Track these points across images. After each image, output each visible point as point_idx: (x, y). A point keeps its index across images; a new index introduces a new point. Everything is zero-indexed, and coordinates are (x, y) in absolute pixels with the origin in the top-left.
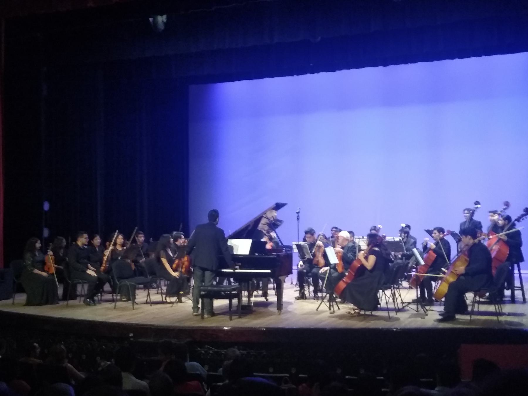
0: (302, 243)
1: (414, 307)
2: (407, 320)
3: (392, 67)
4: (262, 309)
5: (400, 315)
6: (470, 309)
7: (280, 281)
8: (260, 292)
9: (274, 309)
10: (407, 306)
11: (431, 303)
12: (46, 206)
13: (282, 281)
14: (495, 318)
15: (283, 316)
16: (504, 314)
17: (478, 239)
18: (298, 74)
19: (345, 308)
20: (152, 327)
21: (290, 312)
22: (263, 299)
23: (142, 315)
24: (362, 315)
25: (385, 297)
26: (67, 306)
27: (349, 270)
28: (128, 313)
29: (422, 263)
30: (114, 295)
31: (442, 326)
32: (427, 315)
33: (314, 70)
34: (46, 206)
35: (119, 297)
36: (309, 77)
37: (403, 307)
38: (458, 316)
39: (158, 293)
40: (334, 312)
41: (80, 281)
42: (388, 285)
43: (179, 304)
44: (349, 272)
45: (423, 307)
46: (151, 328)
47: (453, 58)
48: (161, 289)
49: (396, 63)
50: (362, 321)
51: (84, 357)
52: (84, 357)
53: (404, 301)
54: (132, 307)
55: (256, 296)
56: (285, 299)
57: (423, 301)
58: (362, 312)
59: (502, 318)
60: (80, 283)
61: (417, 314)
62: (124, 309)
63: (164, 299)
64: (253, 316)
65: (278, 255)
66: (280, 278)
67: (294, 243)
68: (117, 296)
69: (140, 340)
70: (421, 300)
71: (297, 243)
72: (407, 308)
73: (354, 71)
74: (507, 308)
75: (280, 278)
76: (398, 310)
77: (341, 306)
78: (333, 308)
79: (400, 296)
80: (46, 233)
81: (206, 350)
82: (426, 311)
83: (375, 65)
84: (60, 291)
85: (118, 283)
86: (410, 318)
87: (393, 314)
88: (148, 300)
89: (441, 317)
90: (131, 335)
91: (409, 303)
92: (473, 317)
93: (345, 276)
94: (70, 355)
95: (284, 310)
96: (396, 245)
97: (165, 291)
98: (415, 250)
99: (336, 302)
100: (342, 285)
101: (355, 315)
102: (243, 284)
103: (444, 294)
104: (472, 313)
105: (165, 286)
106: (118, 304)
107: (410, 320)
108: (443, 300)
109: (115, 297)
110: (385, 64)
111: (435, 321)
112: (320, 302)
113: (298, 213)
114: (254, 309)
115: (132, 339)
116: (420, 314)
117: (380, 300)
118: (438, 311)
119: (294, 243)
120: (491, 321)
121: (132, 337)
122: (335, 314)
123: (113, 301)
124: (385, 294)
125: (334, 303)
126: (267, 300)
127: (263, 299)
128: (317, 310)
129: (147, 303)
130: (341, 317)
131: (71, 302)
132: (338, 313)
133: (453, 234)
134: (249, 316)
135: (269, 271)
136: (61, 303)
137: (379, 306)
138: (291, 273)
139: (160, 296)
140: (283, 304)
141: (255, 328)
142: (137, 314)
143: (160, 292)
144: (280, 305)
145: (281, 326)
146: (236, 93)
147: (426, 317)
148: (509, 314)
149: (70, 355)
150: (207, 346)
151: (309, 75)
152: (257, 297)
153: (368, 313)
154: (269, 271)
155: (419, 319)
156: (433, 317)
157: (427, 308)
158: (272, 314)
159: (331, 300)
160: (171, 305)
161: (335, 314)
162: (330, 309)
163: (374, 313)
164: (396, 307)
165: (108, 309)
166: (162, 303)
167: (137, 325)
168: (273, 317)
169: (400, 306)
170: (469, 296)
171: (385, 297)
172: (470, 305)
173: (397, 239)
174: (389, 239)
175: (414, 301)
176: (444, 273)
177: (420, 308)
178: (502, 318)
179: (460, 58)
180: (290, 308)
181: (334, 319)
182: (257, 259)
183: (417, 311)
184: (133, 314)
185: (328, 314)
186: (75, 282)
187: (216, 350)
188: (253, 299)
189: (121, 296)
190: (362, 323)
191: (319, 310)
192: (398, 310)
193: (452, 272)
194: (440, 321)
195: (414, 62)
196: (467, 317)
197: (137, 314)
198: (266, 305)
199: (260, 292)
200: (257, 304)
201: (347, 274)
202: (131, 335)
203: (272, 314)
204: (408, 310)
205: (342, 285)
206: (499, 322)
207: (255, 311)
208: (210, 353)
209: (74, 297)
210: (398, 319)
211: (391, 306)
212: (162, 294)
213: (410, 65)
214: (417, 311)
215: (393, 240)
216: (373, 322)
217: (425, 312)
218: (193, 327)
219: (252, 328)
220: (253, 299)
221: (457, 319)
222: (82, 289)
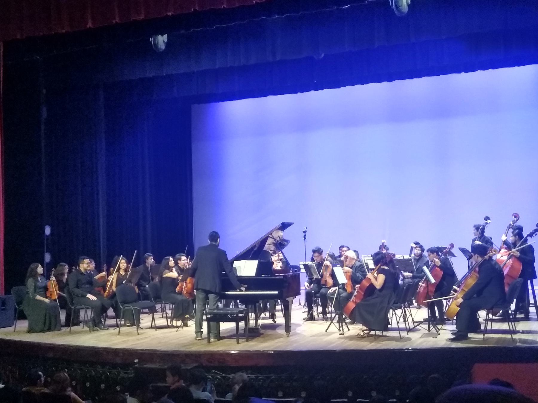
0: (309, 263)
1: (426, 326)
2: (419, 340)
3: (397, 83)
4: (270, 332)
5: (411, 335)
6: (483, 327)
7: (288, 302)
8: (268, 314)
9: (281, 331)
10: (418, 325)
11: (442, 321)
12: (48, 231)
13: (290, 303)
14: (509, 336)
15: (292, 339)
16: (518, 332)
17: (488, 255)
18: (302, 92)
19: (356, 329)
22: (270, 321)
24: (372, 335)
25: (395, 317)
26: (70, 333)
28: (134, 338)
29: (433, 281)
30: (118, 320)
31: (455, 345)
32: (439, 334)
33: (318, 87)
34: (48, 231)
35: (123, 322)
36: (313, 93)
37: (415, 327)
38: (470, 335)
39: (162, 317)
40: (344, 334)
41: (83, 306)
42: (399, 304)
43: (185, 328)
45: (435, 326)
46: (156, 354)
47: (459, 72)
48: (166, 313)
49: (402, 78)
50: (371, 342)
51: (88, 384)
52: (88, 384)
53: (415, 320)
54: (136, 332)
55: (263, 319)
57: (435, 321)
58: (373, 333)
59: (516, 336)
60: (83, 308)
61: (429, 334)
62: (128, 334)
64: (259, 339)
66: (287, 299)
67: (301, 263)
68: (121, 321)
69: (145, 366)
70: (433, 319)
72: (418, 327)
73: (358, 87)
74: (521, 326)
75: (287, 299)
76: (409, 330)
77: (350, 327)
78: (343, 329)
79: (411, 315)
80: (48, 258)
81: (213, 375)
82: (438, 330)
83: (379, 80)
84: (63, 317)
85: (121, 307)
86: (421, 337)
87: (404, 334)
88: (153, 324)
89: (454, 336)
90: (136, 361)
91: (420, 323)
92: (487, 336)
94: (74, 383)
96: (406, 264)
97: (170, 315)
98: (425, 268)
99: (346, 323)
100: (351, 305)
101: (365, 335)
103: (456, 312)
104: (486, 331)
106: (123, 329)
107: (422, 340)
108: (455, 318)
109: (119, 323)
110: (390, 80)
111: (447, 340)
112: (329, 323)
113: (305, 232)
114: (262, 331)
115: (137, 365)
116: (432, 333)
117: (390, 320)
118: (451, 331)
120: (505, 340)
121: (136, 363)
123: (117, 326)
124: (396, 314)
125: (344, 324)
126: (275, 322)
127: (270, 321)
128: (326, 331)
129: (152, 327)
130: (351, 338)
131: (74, 328)
132: (348, 334)
133: (464, 251)
134: (256, 339)
135: (276, 292)
136: (64, 329)
137: (389, 326)
138: (298, 293)
139: (166, 320)
141: (263, 351)
142: (142, 339)
143: (165, 315)
144: (288, 327)
145: (290, 348)
146: (238, 111)
147: (438, 336)
148: (523, 332)
149: (74, 383)
150: (213, 371)
151: (313, 92)
152: (265, 320)
153: (378, 333)
154: (276, 292)
155: (431, 339)
156: (444, 337)
157: (439, 327)
159: (341, 321)
160: (176, 329)
161: (345, 335)
162: (339, 330)
163: (385, 333)
164: (408, 327)
165: (112, 334)
166: (168, 327)
167: (142, 350)
168: (281, 339)
169: (412, 326)
170: (482, 314)
171: (395, 317)
172: (483, 323)
173: (407, 257)
174: (398, 257)
175: (425, 321)
176: (455, 291)
177: (432, 327)
178: (516, 336)
179: (466, 71)
180: (299, 330)
181: (343, 340)
182: (264, 280)
183: (429, 330)
184: (138, 340)
185: (337, 335)
187: (224, 375)
188: (260, 322)
189: (125, 321)
190: (373, 343)
192: (409, 330)
193: (462, 289)
194: (452, 340)
195: (419, 76)
196: (481, 336)
197: (142, 339)
198: (273, 327)
199: (268, 314)
200: (265, 327)
202: (136, 361)
203: (280, 336)
204: (420, 330)
205: (351, 305)
206: (514, 340)
207: (263, 334)
208: (218, 378)
209: (77, 324)
210: (409, 339)
211: (402, 325)
212: (167, 318)
213: (416, 80)
214: (429, 330)
215: (402, 258)
216: (384, 342)
217: (437, 332)
218: (199, 352)
220: (260, 322)
221: (471, 338)
222: (86, 314)
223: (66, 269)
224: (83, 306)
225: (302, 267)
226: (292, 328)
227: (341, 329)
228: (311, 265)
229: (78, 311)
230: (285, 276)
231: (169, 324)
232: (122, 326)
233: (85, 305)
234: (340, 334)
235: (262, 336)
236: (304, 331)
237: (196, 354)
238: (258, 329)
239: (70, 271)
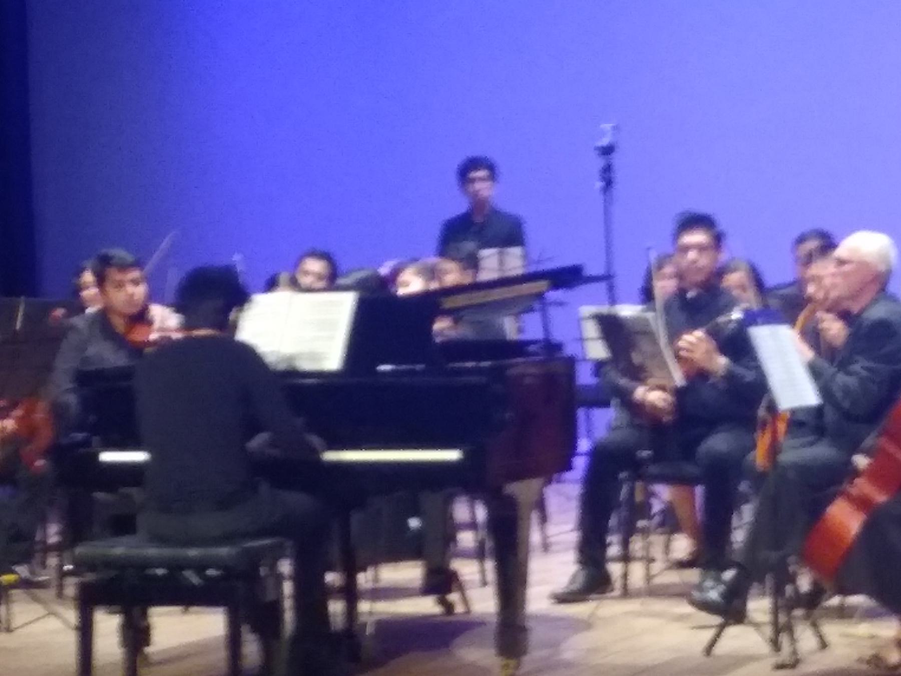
0: (628, 311)
8: (411, 572)
9: (479, 653)
21: (568, 665)
27: (869, 441)
44: (868, 453)
56: (538, 599)
65: (498, 373)
67: (587, 310)
71: (605, 309)
78: (793, 640)
93: (855, 473)
95: (534, 656)
100: (845, 518)
119: (587, 310)
122: (804, 668)
128: (709, 649)
135: (452, 455)
140: (530, 624)
144: (512, 631)
154: (452, 455)
162: (775, 644)
180: (574, 647)
191: (719, 649)
201: (861, 461)
205: (845, 518)
225: (591, 330)
226: (537, 635)
227: (784, 639)
228: (635, 320)
230: (498, 373)
234: (780, 667)
236: (594, 650)
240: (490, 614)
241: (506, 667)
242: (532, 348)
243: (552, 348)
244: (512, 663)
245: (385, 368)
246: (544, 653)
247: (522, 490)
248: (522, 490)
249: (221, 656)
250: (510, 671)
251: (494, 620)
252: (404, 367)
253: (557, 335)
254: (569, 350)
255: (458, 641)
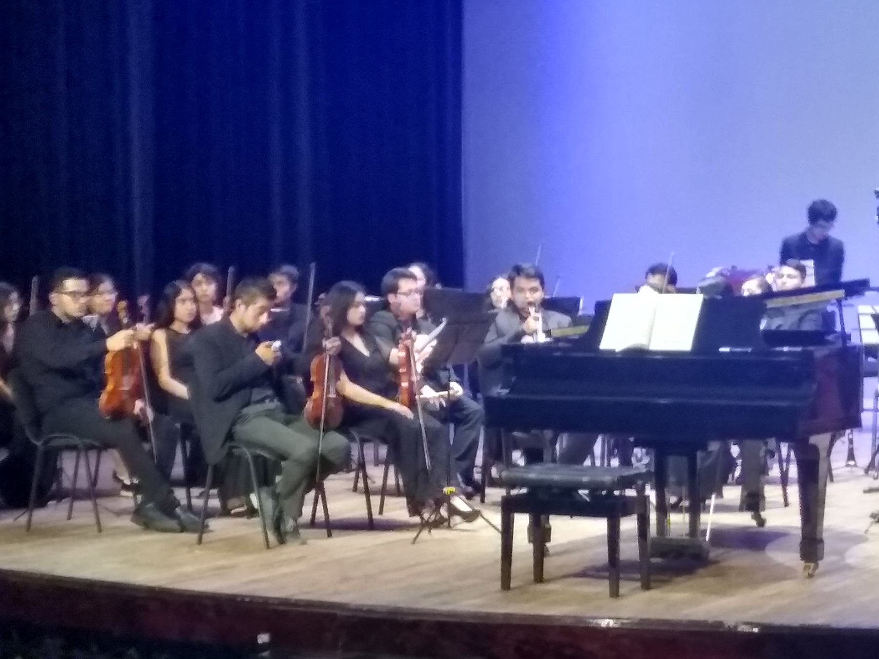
7: (815, 449)
9: (788, 557)
13: (823, 454)
15: (825, 584)
20: (339, 612)
21: (850, 568)
22: (745, 519)
23: (296, 567)
30: (195, 491)
35: (215, 503)
41: (75, 440)
46: (332, 617)
48: (366, 477)
54: (261, 538)
55: (720, 509)
62: (236, 545)
63: (375, 510)
64: (710, 581)
66: (814, 440)
68: (206, 496)
75: (814, 440)
88: (320, 514)
90: (263, 638)
97: (379, 483)
102: (676, 463)
105: (377, 463)
109: (197, 503)
114: (714, 554)
121: (264, 647)
126: (761, 522)
127: (745, 519)
138: (854, 422)
139: (362, 499)
140: (825, 535)
143: (361, 485)
144: (811, 544)
145: (819, 618)
152: (724, 513)
158: (781, 574)
160: (410, 535)
165: (183, 544)
166: (370, 525)
167: (285, 602)
168: (787, 586)
180: (855, 555)
186: (55, 443)
188: (710, 520)
198: (755, 540)
199: (733, 494)
200: (723, 538)
203: (781, 574)
207: (715, 562)
212: (367, 492)
218: (488, 616)
219: (704, 623)
220: (710, 520)
223: (10, 303)
224: (75, 440)
226: (828, 546)
229: (52, 456)
231: (376, 516)
232: (209, 514)
233: (81, 436)
235: (713, 567)
237: (474, 626)
238: (700, 547)
239: (23, 315)
240: (796, 528)
241: (805, 568)
242: (830, 338)
243: (846, 337)
244: (812, 565)
245: (722, 350)
246: (834, 558)
247: (820, 440)
248: (820, 440)
249: (603, 551)
250: (810, 571)
251: (799, 532)
252: (738, 350)
253: (847, 331)
254: (854, 341)
255: (769, 547)
